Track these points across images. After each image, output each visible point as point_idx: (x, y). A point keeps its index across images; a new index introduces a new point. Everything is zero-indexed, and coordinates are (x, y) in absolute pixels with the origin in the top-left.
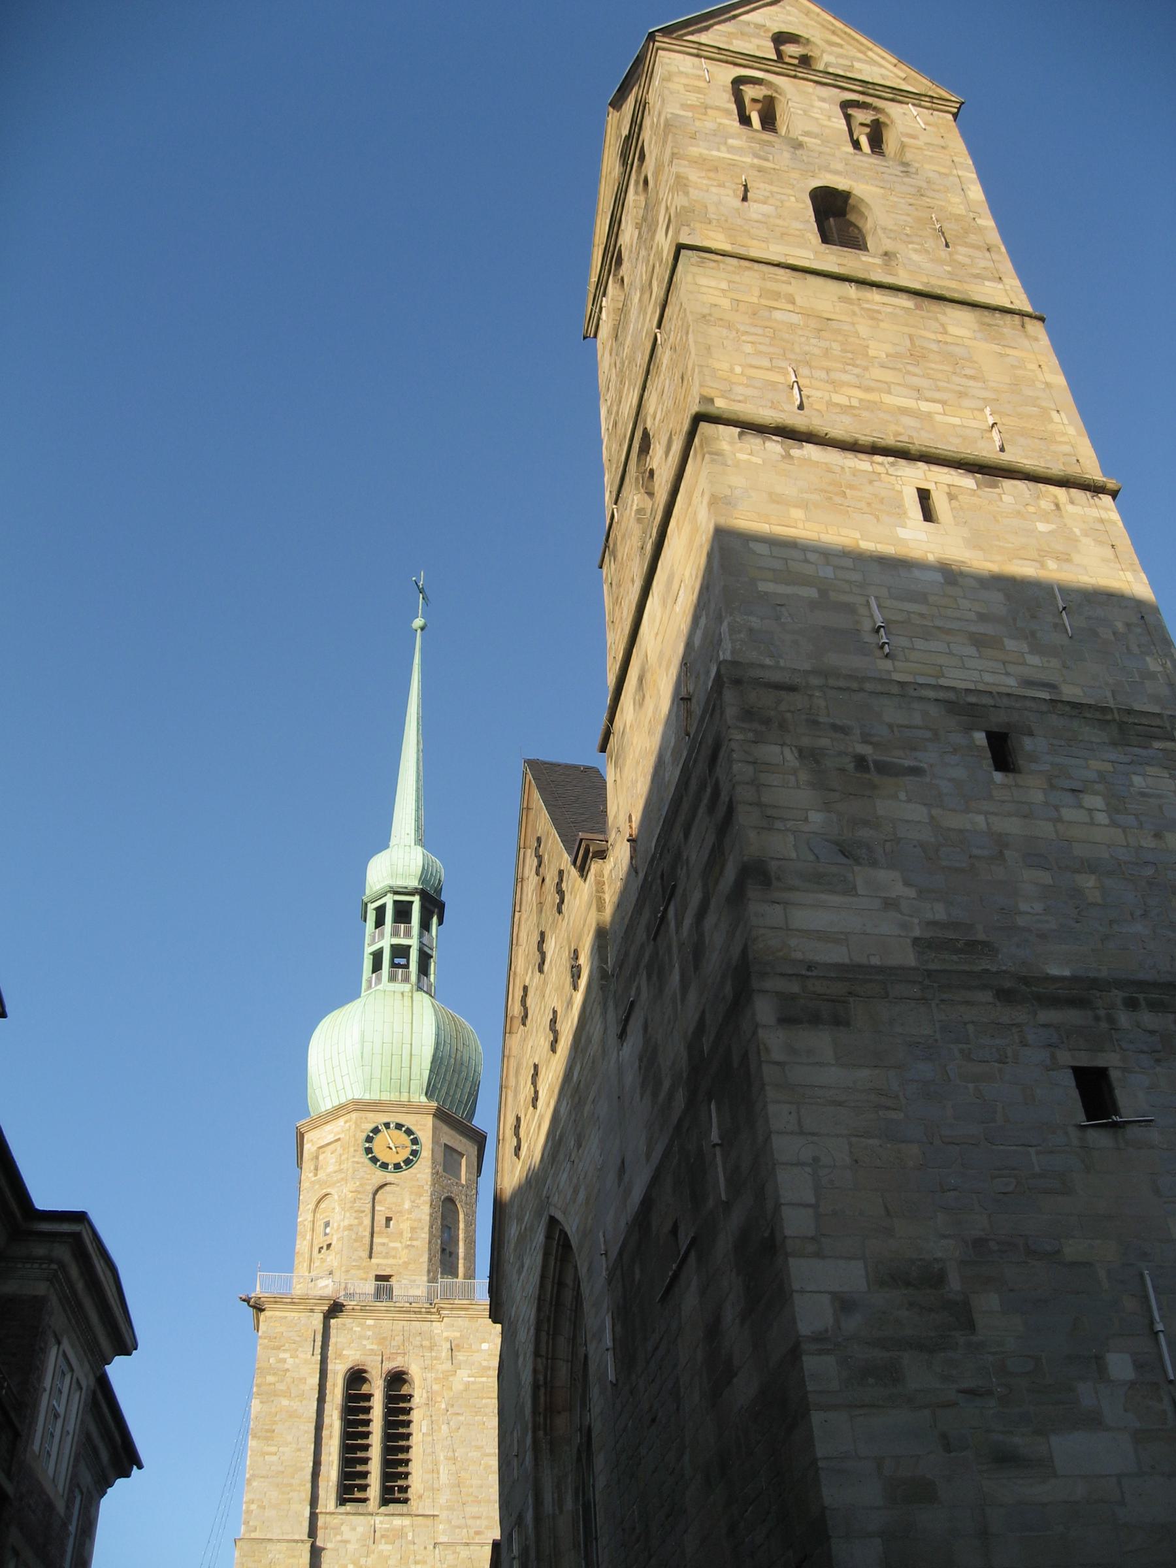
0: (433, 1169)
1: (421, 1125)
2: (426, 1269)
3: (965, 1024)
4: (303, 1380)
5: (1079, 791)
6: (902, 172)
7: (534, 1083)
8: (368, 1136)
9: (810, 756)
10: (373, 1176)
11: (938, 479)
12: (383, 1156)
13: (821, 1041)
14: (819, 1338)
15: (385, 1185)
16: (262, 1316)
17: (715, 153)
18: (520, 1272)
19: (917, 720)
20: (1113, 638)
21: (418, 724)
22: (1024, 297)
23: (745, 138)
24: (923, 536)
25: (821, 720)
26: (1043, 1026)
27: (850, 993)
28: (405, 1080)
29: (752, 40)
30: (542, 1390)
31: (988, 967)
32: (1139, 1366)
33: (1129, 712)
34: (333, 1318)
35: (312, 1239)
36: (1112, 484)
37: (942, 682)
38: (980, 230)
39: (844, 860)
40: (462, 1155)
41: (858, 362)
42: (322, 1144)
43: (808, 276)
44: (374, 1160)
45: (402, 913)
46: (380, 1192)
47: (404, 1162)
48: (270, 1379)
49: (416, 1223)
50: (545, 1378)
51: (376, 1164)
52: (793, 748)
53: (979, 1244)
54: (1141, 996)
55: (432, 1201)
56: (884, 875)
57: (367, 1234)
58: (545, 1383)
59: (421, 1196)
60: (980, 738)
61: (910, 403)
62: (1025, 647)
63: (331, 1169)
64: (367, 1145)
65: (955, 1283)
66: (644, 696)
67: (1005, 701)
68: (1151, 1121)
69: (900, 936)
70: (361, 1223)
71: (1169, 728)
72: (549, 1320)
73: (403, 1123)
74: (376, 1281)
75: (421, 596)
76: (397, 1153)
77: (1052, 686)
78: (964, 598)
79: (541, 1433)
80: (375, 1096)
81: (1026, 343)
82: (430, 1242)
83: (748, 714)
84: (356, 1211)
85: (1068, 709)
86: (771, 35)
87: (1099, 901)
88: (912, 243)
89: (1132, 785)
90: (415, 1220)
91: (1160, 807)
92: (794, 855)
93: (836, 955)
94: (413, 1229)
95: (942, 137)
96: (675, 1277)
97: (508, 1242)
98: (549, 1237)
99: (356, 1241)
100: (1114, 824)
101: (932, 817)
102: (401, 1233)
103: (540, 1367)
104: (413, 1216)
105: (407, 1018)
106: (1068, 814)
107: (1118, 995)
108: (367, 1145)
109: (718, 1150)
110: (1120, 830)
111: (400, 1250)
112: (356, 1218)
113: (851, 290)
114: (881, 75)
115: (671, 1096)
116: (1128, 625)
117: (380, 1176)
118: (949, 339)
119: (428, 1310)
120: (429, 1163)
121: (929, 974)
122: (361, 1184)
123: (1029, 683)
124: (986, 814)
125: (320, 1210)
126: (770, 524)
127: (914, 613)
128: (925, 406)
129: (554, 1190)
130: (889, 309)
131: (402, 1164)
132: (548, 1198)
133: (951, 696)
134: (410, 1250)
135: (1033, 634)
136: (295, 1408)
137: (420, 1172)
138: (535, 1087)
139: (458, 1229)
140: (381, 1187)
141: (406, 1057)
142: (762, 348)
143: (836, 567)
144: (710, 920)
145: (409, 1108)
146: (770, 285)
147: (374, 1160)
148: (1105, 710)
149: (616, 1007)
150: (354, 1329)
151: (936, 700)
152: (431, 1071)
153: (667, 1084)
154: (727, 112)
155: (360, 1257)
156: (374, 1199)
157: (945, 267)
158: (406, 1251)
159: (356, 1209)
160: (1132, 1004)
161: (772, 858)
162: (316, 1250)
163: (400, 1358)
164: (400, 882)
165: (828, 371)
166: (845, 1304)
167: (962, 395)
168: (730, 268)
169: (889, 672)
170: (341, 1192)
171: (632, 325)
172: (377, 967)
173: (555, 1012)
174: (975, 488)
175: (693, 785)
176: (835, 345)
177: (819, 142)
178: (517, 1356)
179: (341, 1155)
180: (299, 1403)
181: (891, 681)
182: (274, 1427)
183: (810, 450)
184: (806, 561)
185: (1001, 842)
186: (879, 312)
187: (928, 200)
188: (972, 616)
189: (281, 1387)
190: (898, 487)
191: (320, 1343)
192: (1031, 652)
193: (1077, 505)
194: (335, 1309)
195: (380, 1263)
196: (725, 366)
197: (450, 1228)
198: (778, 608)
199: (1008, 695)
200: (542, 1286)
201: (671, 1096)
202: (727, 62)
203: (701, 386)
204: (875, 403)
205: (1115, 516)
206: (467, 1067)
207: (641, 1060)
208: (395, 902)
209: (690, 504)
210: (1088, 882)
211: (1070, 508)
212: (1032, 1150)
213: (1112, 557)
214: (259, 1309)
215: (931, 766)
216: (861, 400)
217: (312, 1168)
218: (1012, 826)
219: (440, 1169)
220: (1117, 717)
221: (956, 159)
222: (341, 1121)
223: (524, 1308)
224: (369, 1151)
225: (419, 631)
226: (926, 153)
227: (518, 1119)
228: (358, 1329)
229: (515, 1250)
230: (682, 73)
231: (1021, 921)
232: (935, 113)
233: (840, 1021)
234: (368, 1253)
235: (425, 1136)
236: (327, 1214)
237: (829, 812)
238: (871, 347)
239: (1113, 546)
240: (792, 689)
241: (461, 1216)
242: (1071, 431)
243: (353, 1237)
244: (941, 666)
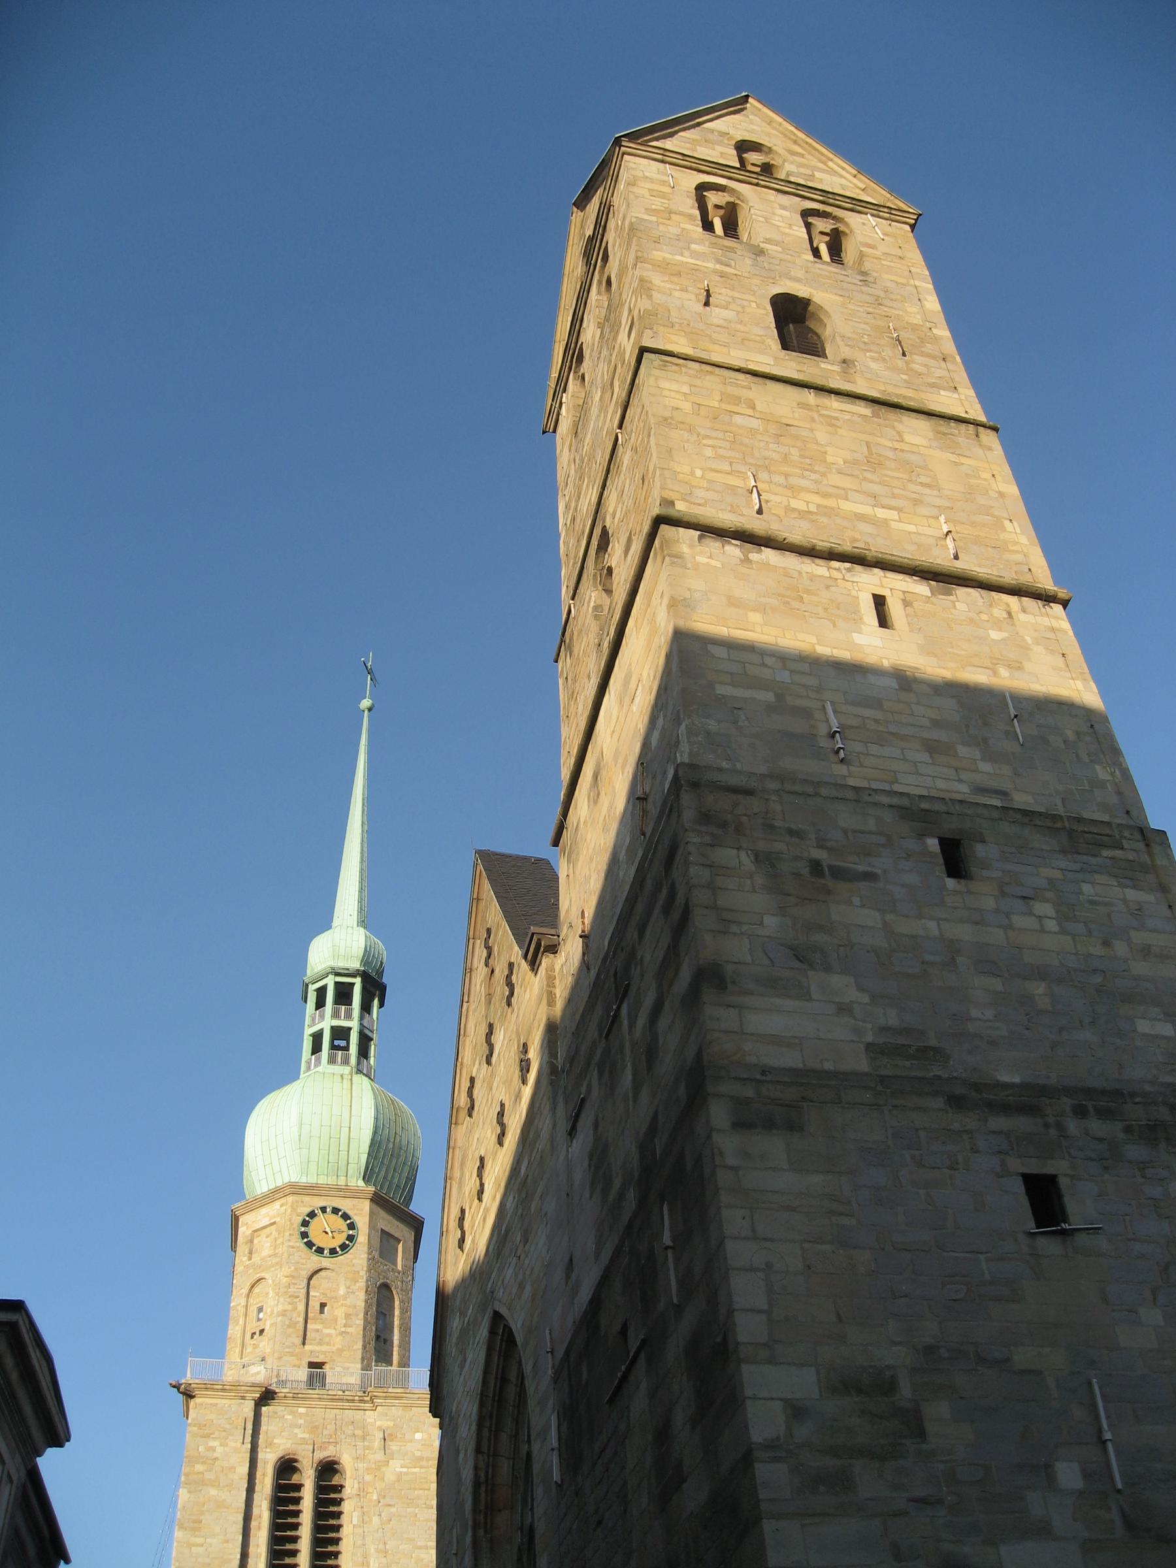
0: (369, 1254)
1: (358, 1209)
2: (360, 1357)
3: (917, 1130)
4: (232, 1469)
5: (1030, 898)
6: (861, 281)
7: (480, 1175)
8: (304, 1220)
9: (765, 860)
10: (308, 1261)
11: (894, 585)
12: (319, 1241)
13: (774, 1146)
14: (771, 1445)
15: (321, 1270)
16: (192, 1403)
17: (678, 258)
18: (462, 1367)
19: (872, 825)
20: (1063, 747)
21: (363, 805)
22: (978, 406)
23: (707, 243)
24: (878, 642)
26: (994, 1132)
27: (803, 1098)
28: (343, 1163)
29: (716, 147)
30: (483, 1488)
31: (939, 1073)
32: (1087, 1475)
33: (1079, 820)
34: (265, 1406)
35: (245, 1324)
36: (1062, 593)
37: (897, 788)
38: (936, 339)
39: (798, 965)
40: (399, 1241)
41: (816, 468)
42: (258, 1227)
43: (768, 382)
44: (310, 1245)
45: (343, 995)
46: (314, 1277)
47: (340, 1247)
48: (199, 1467)
49: (351, 1310)
50: (487, 1473)
51: (311, 1249)
52: (749, 852)
53: (930, 1350)
55: (367, 1287)
56: (837, 980)
57: (301, 1320)
58: (487, 1481)
59: (356, 1281)
60: (933, 844)
61: (866, 510)
62: (977, 754)
63: (266, 1253)
64: (303, 1229)
65: (905, 1391)
66: (599, 794)
68: (1099, 1228)
69: (853, 1041)
70: (295, 1309)
71: (1118, 837)
72: (491, 1417)
73: (340, 1207)
74: (309, 1368)
75: (369, 676)
76: (333, 1238)
77: (1003, 793)
78: (918, 704)
79: (481, 1532)
80: (312, 1180)
81: (980, 452)
82: (364, 1329)
83: (705, 817)
84: (290, 1297)
85: (1019, 816)
86: (734, 142)
88: (870, 351)
89: (1081, 893)
90: (350, 1307)
91: (1109, 915)
92: (748, 959)
93: (788, 1059)
94: (347, 1316)
95: (900, 247)
96: (625, 1378)
97: (450, 1335)
98: (493, 1332)
99: (289, 1326)
101: (885, 923)
102: (335, 1320)
103: (482, 1465)
104: (348, 1302)
106: (1019, 921)
107: (1067, 1102)
108: (303, 1229)
109: (670, 1253)
110: (1069, 938)
111: (334, 1336)
112: (290, 1304)
113: (810, 397)
114: (841, 185)
115: (621, 1196)
116: (1078, 734)
117: (315, 1261)
118: (905, 447)
119: (361, 1398)
120: (366, 1249)
121: (882, 1079)
122: (296, 1269)
124: (938, 920)
126: (728, 628)
127: (868, 718)
128: (881, 513)
129: (499, 1283)
130: (847, 417)
131: (338, 1249)
132: (493, 1292)
133: (905, 802)
134: (344, 1337)
135: (985, 740)
136: (223, 1497)
137: (355, 1258)
138: (481, 1179)
139: (394, 1316)
140: (316, 1272)
141: (344, 1140)
142: (721, 451)
143: (792, 672)
144: (663, 1023)
145: (346, 1192)
146: (730, 389)
147: (310, 1245)
148: (1056, 818)
149: (566, 1102)
150: (286, 1417)
151: (891, 806)
153: (617, 1183)
154: (690, 217)
155: (293, 1343)
156: (308, 1284)
157: (902, 376)
159: (290, 1294)
160: (1080, 1112)
161: (727, 962)
162: (248, 1335)
163: (331, 1448)
164: (341, 964)
165: (786, 476)
166: (797, 1411)
167: (917, 502)
168: (691, 372)
169: (844, 777)
170: (275, 1277)
171: (592, 423)
172: (316, 1048)
173: (502, 1105)
174: (930, 595)
175: (649, 884)
176: (794, 451)
177: (780, 249)
178: (458, 1452)
179: (276, 1239)
180: (228, 1493)
181: (846, 786)
182: (202, 1517)
183: (768, 554)
184: (764, 665)
186: (836, 419)
187: (886, 309)
189: (210, 1476)
190: (854, 593)
191: (251, 1432)
193: (1029, 614)
194: (267, 1397)
195: (315, 1351)
196: (686, 469)
197: (385, 1315)
198: (735, 711)
199: (961, 801)
200: (485, 1382)
201: (621, 1196)
202: (691, 168)
203: (662, 488)
204: (833, 509)
205: (1065, 625)
206: (406, 1151)
207: (591, 1157)
208: (336, 983)
209: (649, 605)
210: (1039, 989)
211: (1022, 617)
212: (982, 1257)
213: (1063, 666)
214: (189, 1395)
215: (885, 871)
216: (818, 506)
217: (247, 1251)
218: (962, 932)
220: (1067, 825)
221: (913, 269)
222: (277, 1205)
223: (466, 1405)
224: (304, 1235)
225: (366, 712)
226: (884, 262)
227: (463, 1211)
228: (290, 1417)
229: (457, 1344)
230: (647, 177)
232: (893, 223)
233: (794, 1126)
234: (301, 1339)
236: (261, 1299)
237: (785, 916)
238: (829, 453)
239: (1063, 654)
240: (749, 792)
241: (397, 1303)
242: (1024, 540)
243: (287, 1323)
244: (895, 772)
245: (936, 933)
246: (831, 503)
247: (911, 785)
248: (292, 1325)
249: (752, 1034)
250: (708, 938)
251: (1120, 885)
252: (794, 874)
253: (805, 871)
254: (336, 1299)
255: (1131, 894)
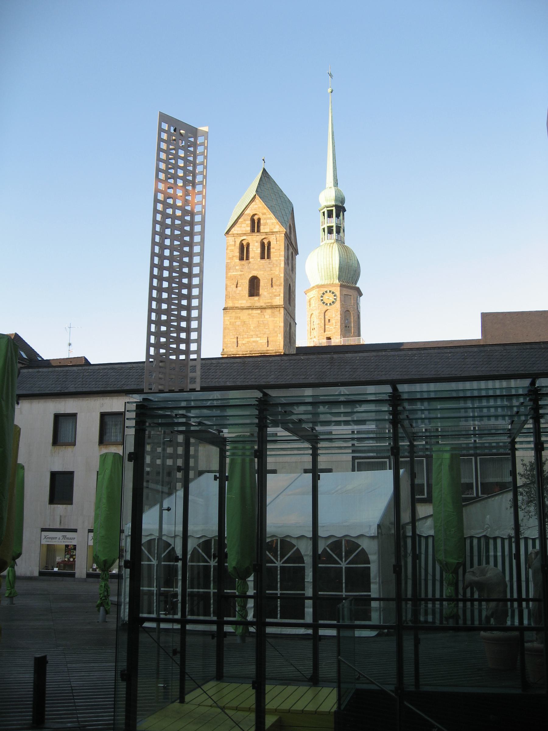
0: (341, 303)
28: (332, 275)
44: (324, 303)
57: (323, 325)
59: (337, 312)
63: (313, 305)
64: (321, 298)
70: (321, 323)
94: (336, 323)
105: (331, 256)
108: (321, 298)
117: (326, 307)
120: (339, 302)
125: (312, 318)
141: (331, 268)
145: (332, 285)
147: (324, 303)
152: (339, 271)
155: (322, 333)
158: (334, 329)
162: (312, 330)
195: (328, 334)
208: (328, 210)
217: (309, 304)
219: (343, 303)
222: (315, 290)
224: (322, 300)
235: (338, 293)
242: (281, 338)
248: (321, 327)
254: (332, 317)
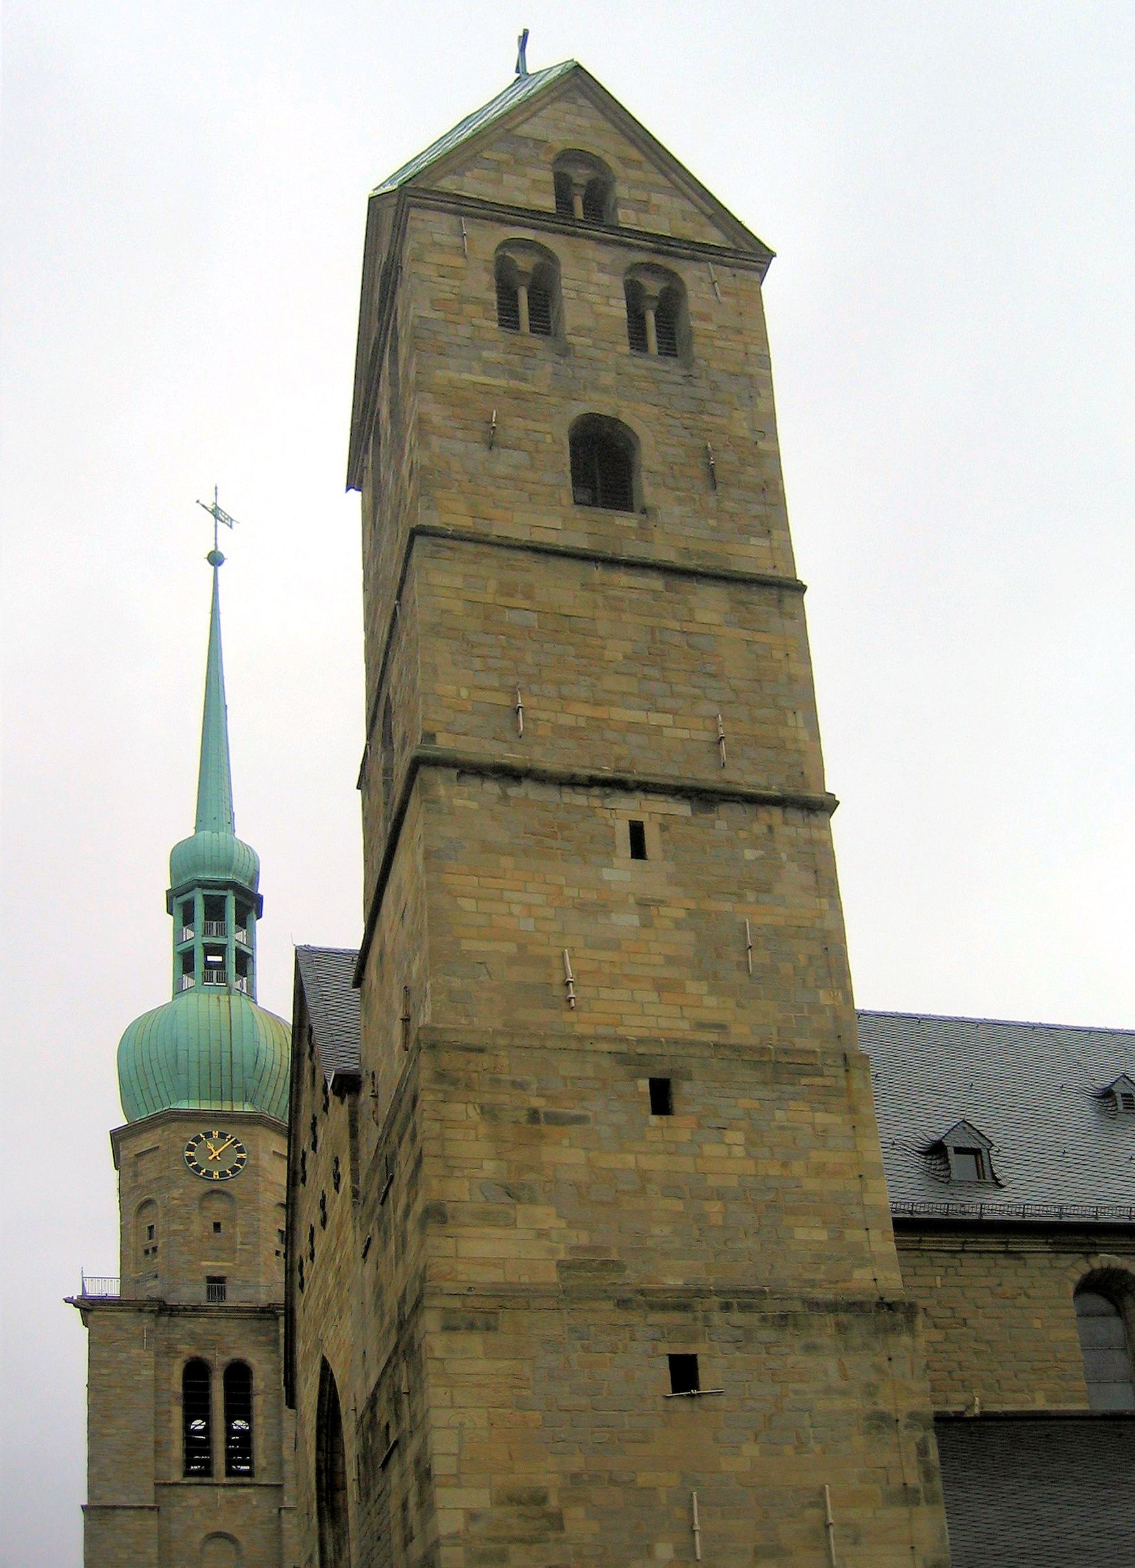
9: (490, 1113)
13: (475, 1342)
19: (589, 1072)
24: (626, 876)
25: (503, 1077)
32: (677, 1551)
37: (621, 1031)
39: (508, 1200)
52: (476, 1106)
53: (575, 1477)
54: (734, 1301)
56: (539, 1211)
60: (644, 1085)
61: (639, 716)
67: (672, 1050)
77: (721, 1027)
83: (441, 1076)
87: (720, 1223)
89: (774, 1120)
92: (467, 1197)
93: (495, 1276)
100: (749, 1155)
101: (589, 1160)
106: (708, 1149)
123: (702, 1026)
133: (623, 1048)
135: (716, 976)
142: (491, 662)
160: (727, 1307)
165: (559, 683)
176: (571, 650)
184: (511, 914)
185: (644, 1176)
188: (660, 960)
190: (611, 822)
192: (710, 994)
210: (714, 1208)
216: (589, 718)
218: (656, 1163)
231: (650, 1243)
237: (500, 1160)
240: (481, 1050)
245: (632, 1166)
246: (599, 713)
247: (634, 1027)
249: (465, 1258)
250: (435, 1182)
251: (814, 1110)
252: (513, 1122)
253: (523, 1119)
255: (821, 1118)
